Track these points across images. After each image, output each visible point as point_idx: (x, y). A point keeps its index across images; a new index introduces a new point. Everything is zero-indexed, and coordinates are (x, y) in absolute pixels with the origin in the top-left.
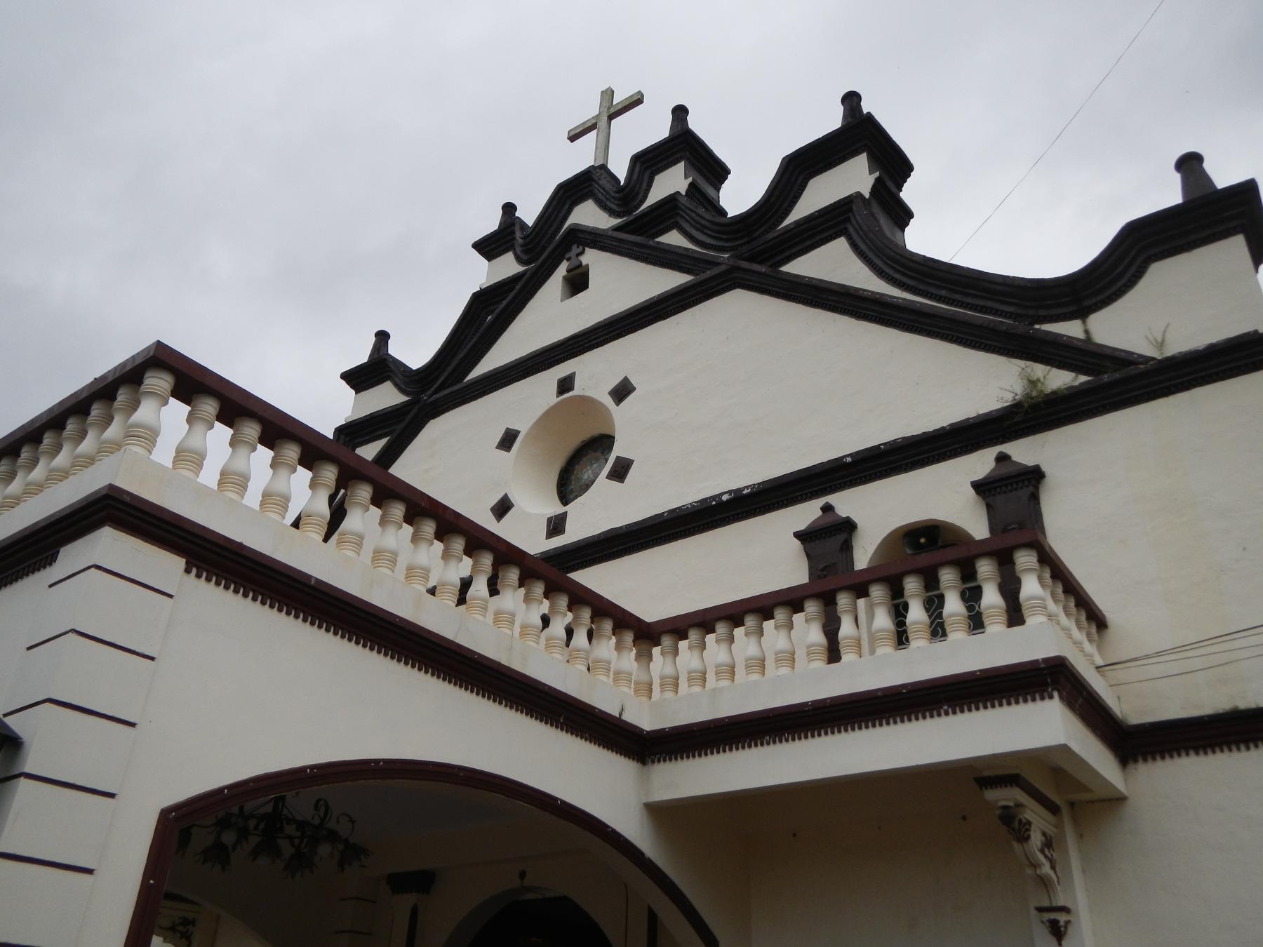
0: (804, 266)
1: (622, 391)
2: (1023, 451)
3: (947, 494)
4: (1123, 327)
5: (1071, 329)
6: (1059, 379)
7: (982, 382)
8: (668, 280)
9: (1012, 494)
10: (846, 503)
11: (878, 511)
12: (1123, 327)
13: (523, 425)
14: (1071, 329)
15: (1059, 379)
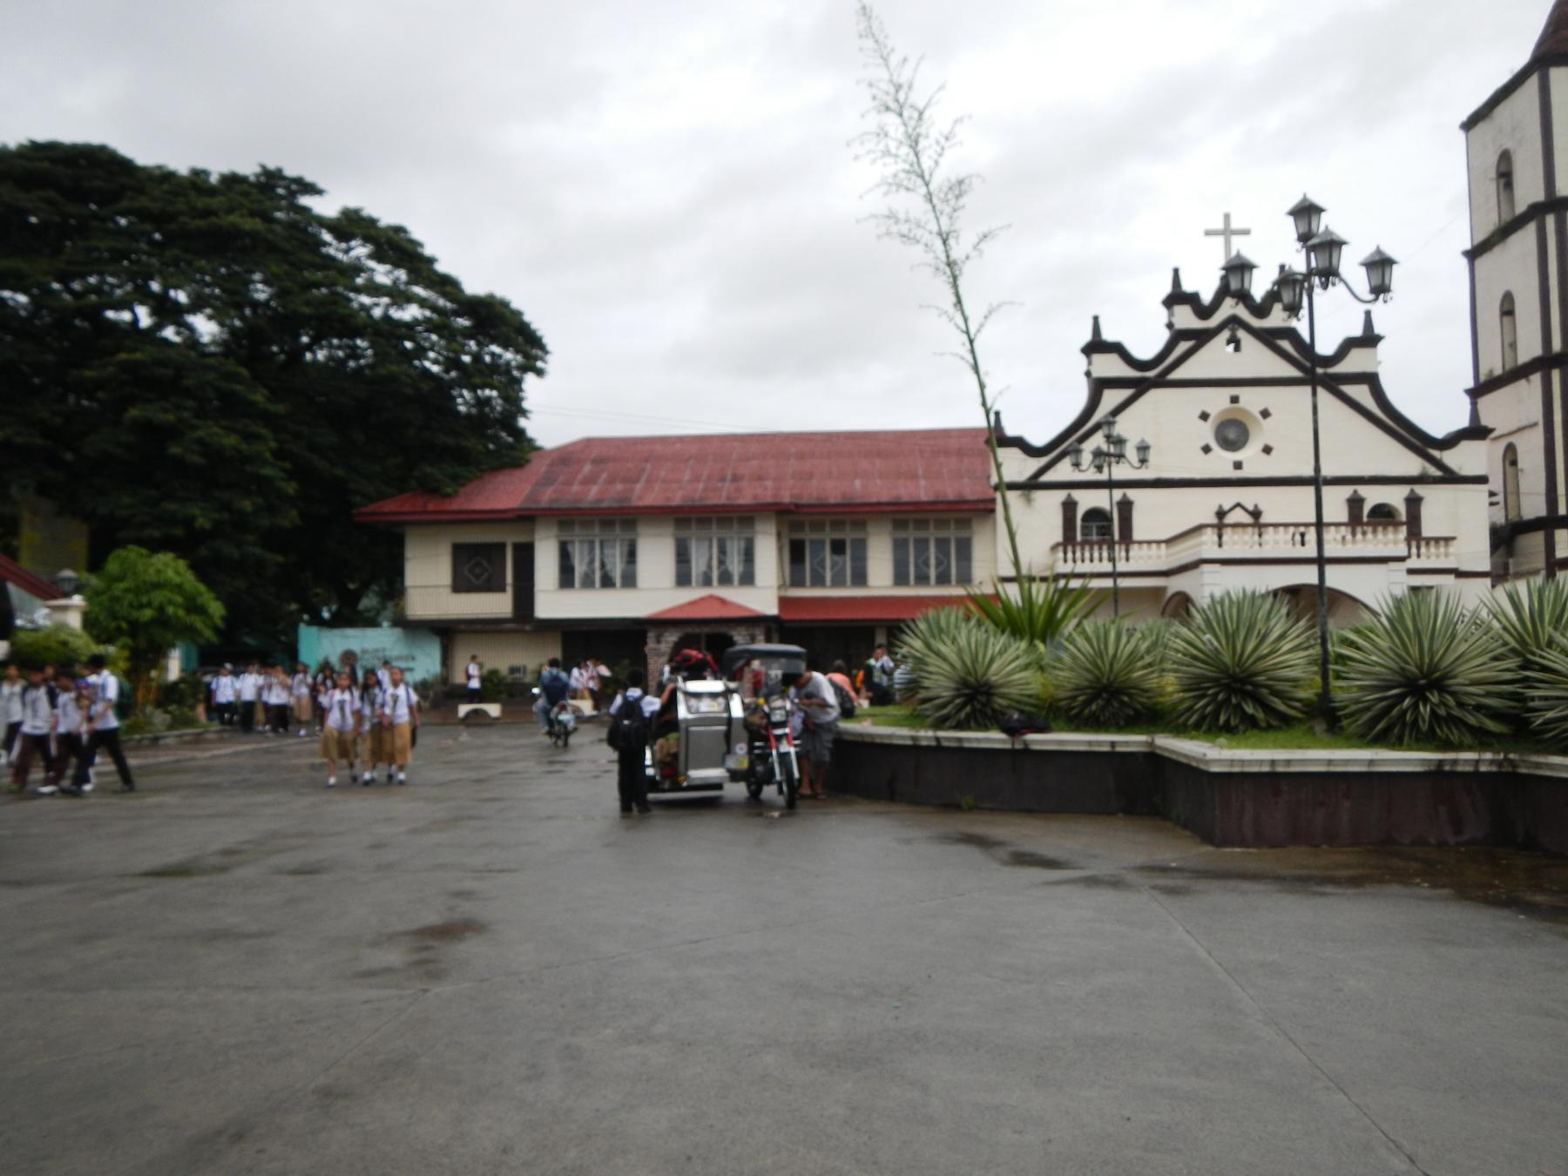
0: (1349, 389)
1: (1265, 414)
2: (1420, 490)
3: (1395, 497)
4: (1451, 458)
5: (1436, 453)
6: (1433, 471)
7: (1411, 464)
8: (1291, 371)
9: (1414, 502)
10: (1363, 491)
11: (1373, 496)
12: (1451, 458)
13: (1214, 412)
14: (1436, 453)
15: (1433, 471)
